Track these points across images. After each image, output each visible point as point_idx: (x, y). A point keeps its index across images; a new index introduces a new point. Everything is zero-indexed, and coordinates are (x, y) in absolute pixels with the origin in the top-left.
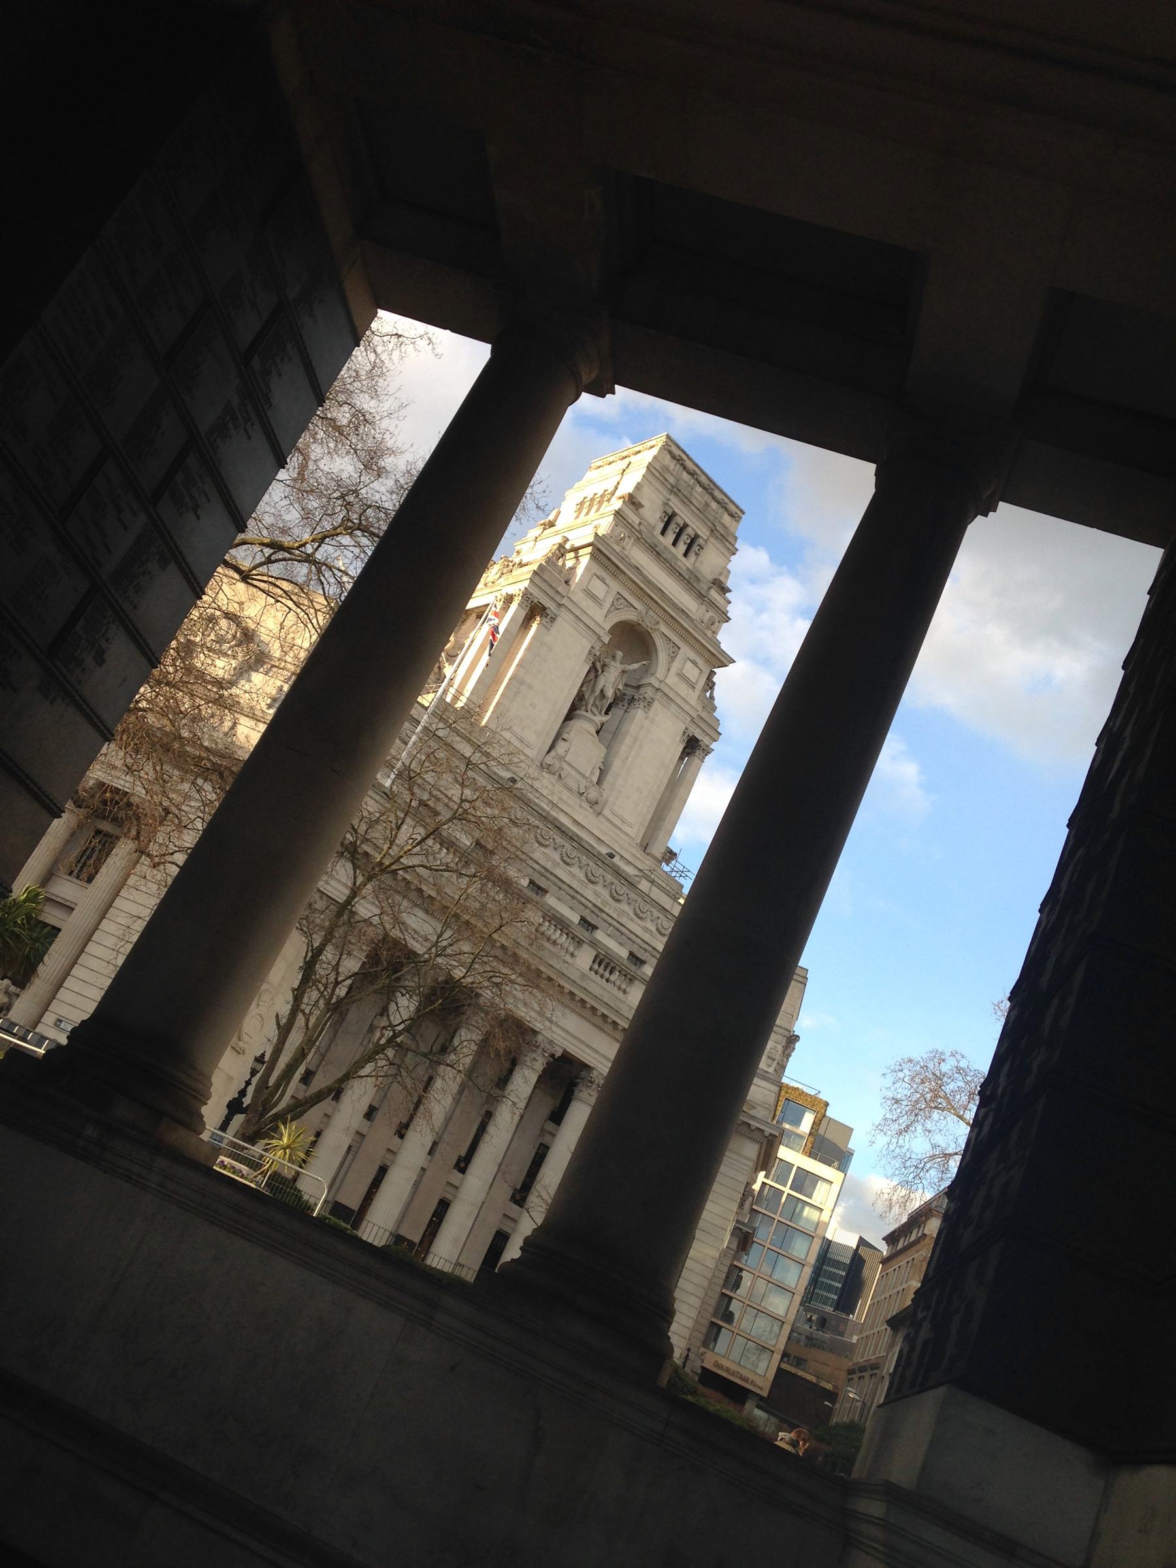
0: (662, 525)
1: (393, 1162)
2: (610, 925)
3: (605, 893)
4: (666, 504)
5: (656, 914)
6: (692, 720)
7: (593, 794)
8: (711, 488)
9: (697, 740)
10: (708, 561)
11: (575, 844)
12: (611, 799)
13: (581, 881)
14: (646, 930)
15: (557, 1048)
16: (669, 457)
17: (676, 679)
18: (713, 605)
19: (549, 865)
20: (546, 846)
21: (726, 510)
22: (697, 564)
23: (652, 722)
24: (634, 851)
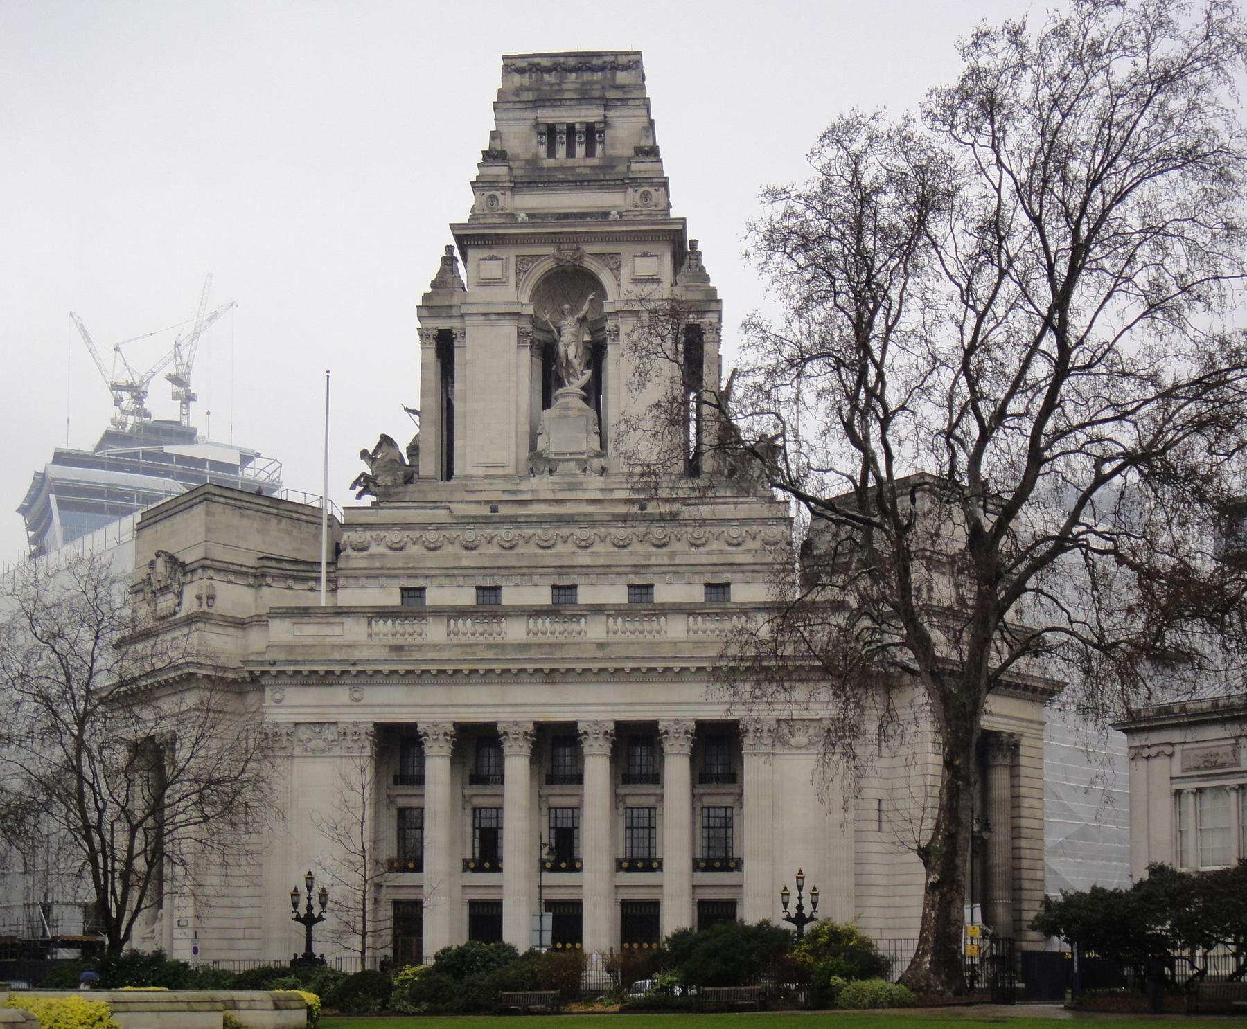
0: (543, 150)
2: (664, 573)
4: (536, 125)
7: (596, 463)
8: (585, 62)
13: (609, 554)
22: (610, 152)
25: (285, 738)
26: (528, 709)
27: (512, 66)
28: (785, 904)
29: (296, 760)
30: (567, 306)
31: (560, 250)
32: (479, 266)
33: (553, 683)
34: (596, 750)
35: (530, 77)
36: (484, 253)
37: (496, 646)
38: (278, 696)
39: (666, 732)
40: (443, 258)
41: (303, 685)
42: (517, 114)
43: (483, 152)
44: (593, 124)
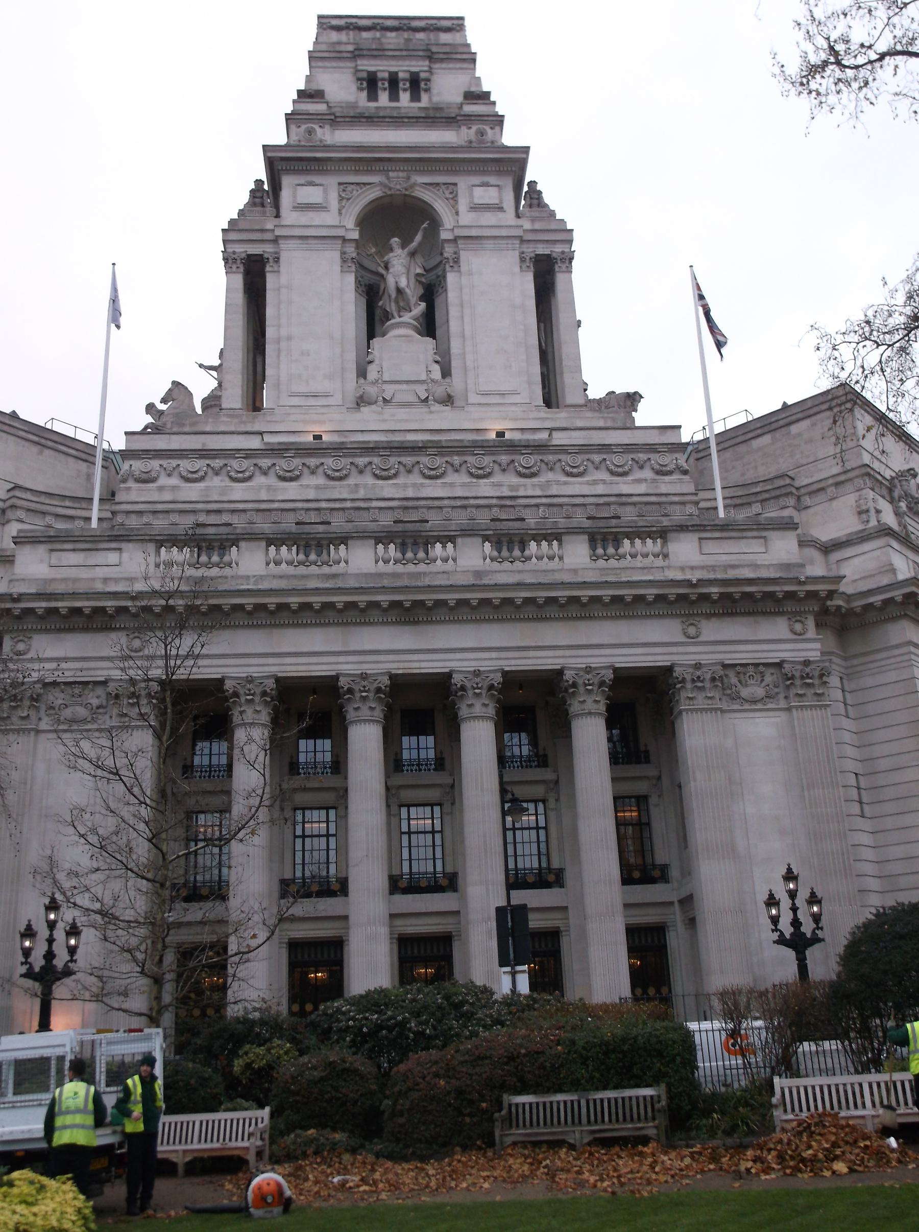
0: (365, 94)
1: (348, 928)
2: (537, 506)
3: (512, 479)
5: (597, 458)
6: (522, 240)
7: (440, 391)
8: (404, 25)
9: (548, 256)
10: (446, 87)
11: (431, 451)
12: (471, 382)
13: (464, 485)
14: (595, 482)
15: (492, 676)
17: (473, 215)
18: (469, 119)
19: (410, 493)
20: (395, 476)
22: (435, 99)
23: (470, 273)
24: (532, 415)
25: (27, 703)
26: (381, 658)
27: (326, 23)
28: (775, 920)
29: (43, 736)
30: (396, 239)
31: (388, 178)
33: (416, 623)
34: (478, 709)
35: (347, 34)
36: (302, 179)
37: (335, 576)
38: (21, 647)
39: (574, 685)
40: (252, 191)
41: (59, 630)
42: (334, 64)
43: (298, 91)
44: (417, 74)
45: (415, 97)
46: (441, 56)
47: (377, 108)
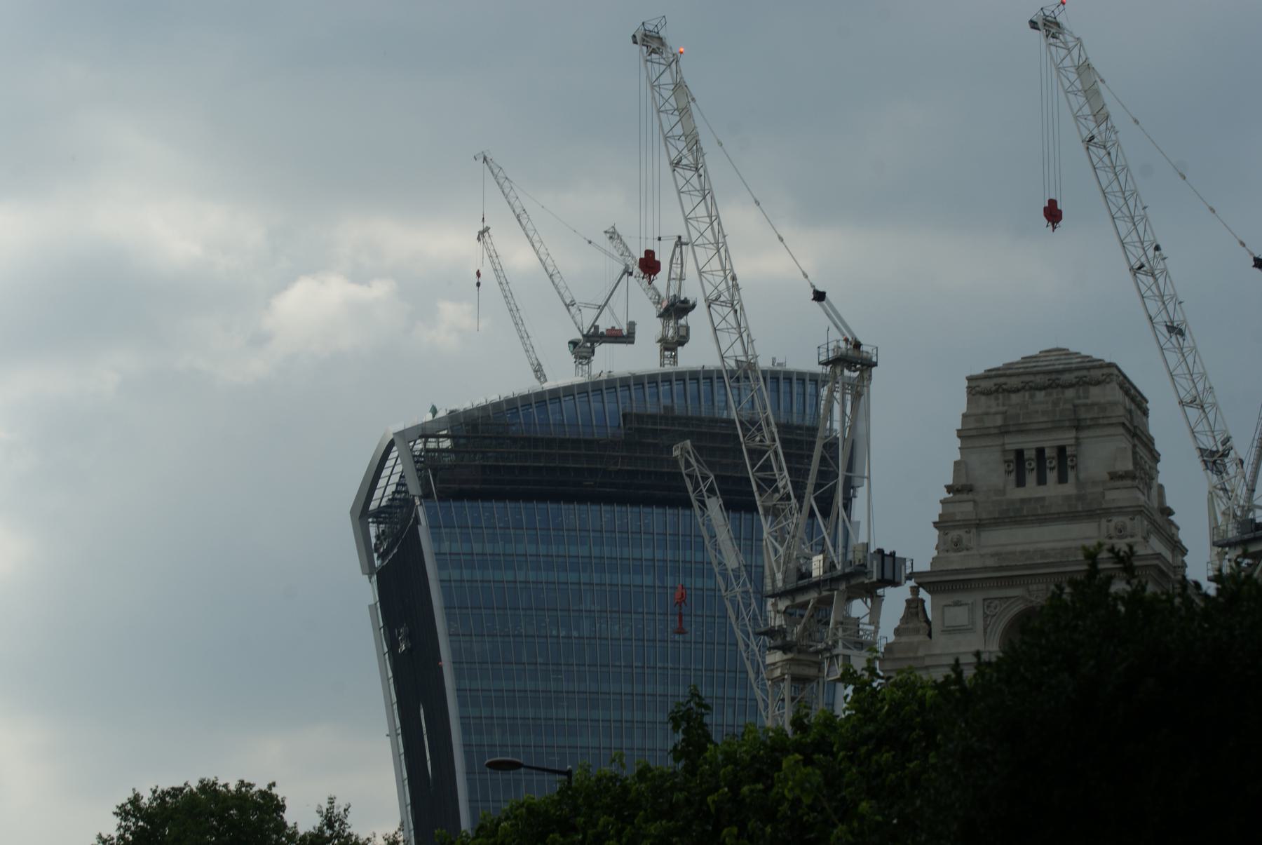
0: (1013, 477)
4: (1004, 452)
16: (983, 398)
21: (1086, 383)
32: (943, 612)
35: (997, 399)
40: (908, 601)
45: (1062, 479)
46: (1088, 423)
47: (1023, 501)
